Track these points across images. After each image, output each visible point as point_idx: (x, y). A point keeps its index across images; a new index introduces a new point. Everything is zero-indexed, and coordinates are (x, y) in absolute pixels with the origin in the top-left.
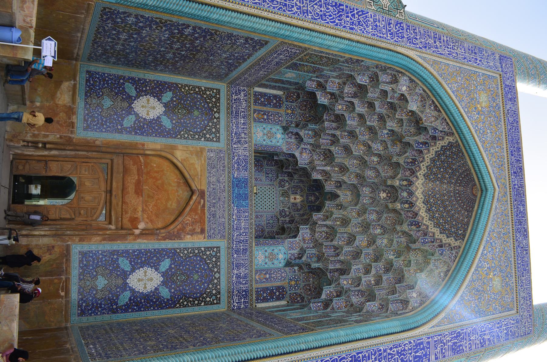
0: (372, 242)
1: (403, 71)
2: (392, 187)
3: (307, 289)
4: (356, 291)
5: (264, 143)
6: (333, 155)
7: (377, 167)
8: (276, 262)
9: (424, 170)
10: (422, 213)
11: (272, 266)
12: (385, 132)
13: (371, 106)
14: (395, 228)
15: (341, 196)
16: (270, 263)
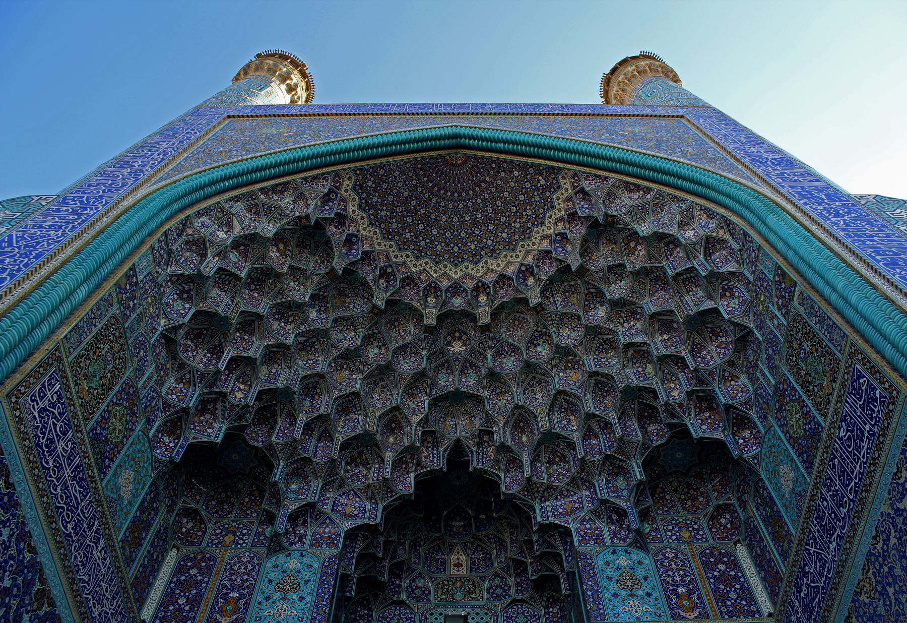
0: (565, 355)
1: (182, 216)
2: (440, 318)
3: (693, 506)
4: (695, 362)
5: (308, 599)
6: (356, 438)
7: (392, 347)
8: (640, 572)
9: (407, 256)
10: (498, 265)
11: (654, 580)
12: (313, 314)
13: (250, 325)
14: (535, 308)
15: (458, 435)
16: (646, 586)
